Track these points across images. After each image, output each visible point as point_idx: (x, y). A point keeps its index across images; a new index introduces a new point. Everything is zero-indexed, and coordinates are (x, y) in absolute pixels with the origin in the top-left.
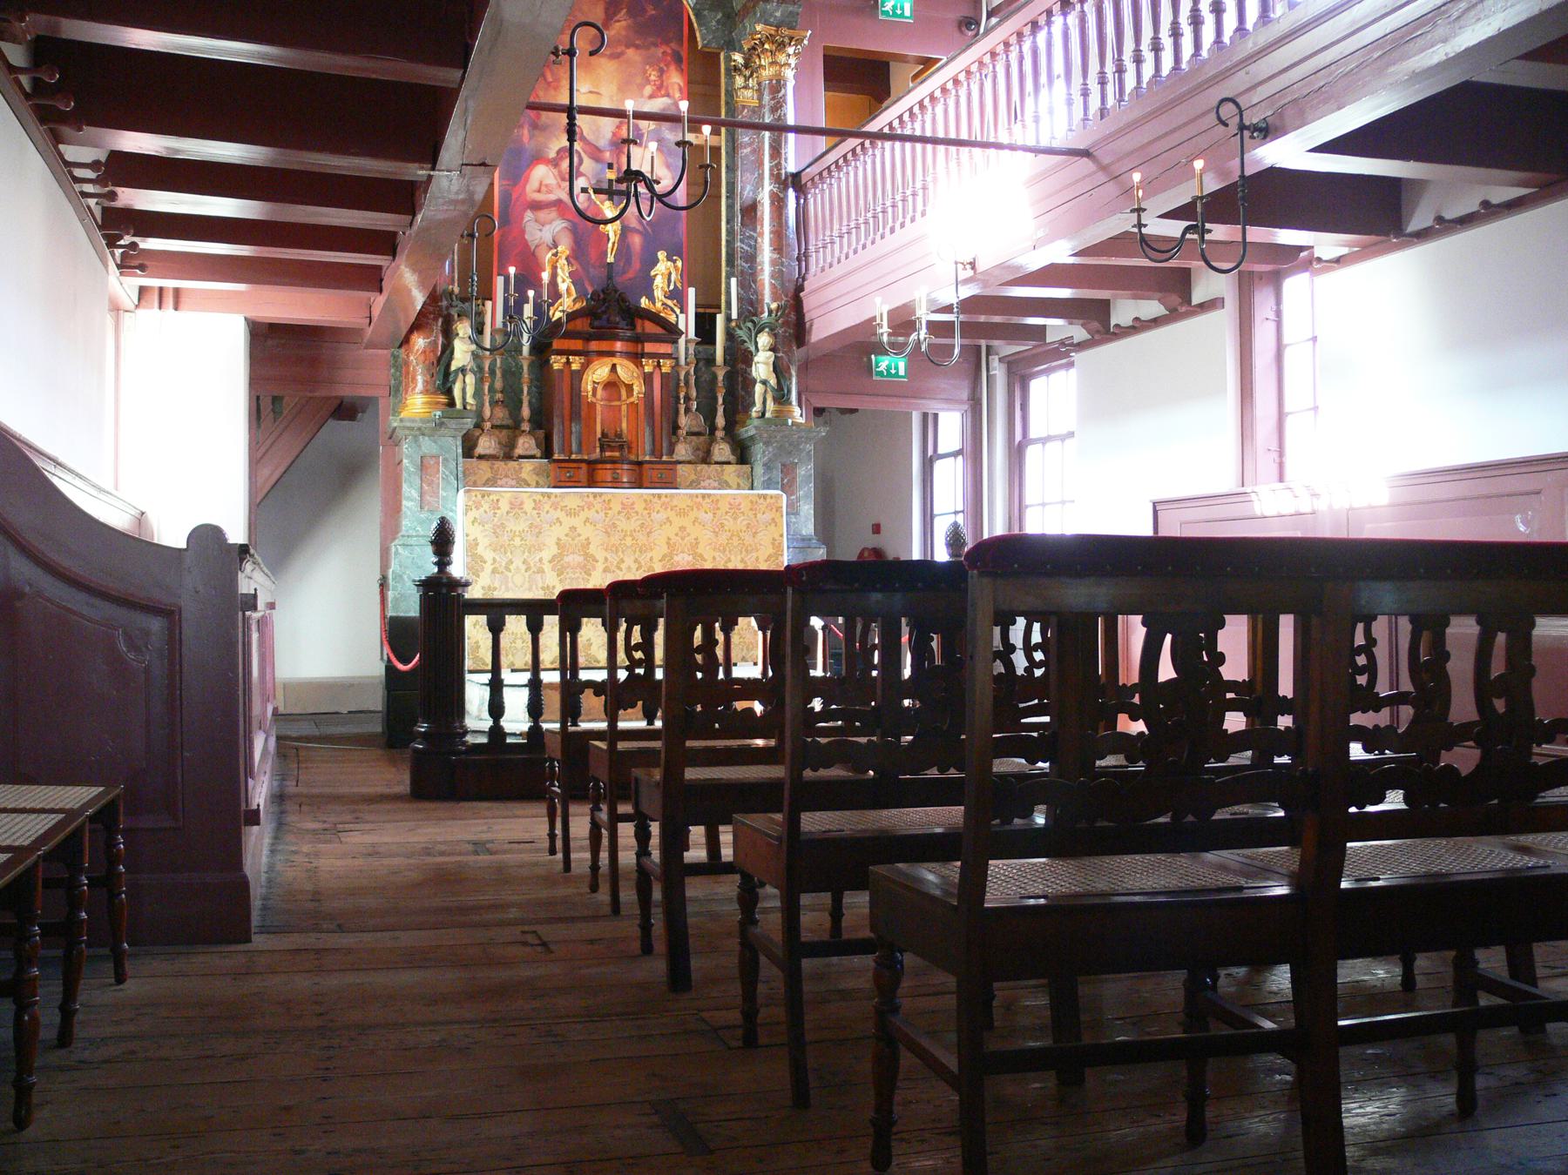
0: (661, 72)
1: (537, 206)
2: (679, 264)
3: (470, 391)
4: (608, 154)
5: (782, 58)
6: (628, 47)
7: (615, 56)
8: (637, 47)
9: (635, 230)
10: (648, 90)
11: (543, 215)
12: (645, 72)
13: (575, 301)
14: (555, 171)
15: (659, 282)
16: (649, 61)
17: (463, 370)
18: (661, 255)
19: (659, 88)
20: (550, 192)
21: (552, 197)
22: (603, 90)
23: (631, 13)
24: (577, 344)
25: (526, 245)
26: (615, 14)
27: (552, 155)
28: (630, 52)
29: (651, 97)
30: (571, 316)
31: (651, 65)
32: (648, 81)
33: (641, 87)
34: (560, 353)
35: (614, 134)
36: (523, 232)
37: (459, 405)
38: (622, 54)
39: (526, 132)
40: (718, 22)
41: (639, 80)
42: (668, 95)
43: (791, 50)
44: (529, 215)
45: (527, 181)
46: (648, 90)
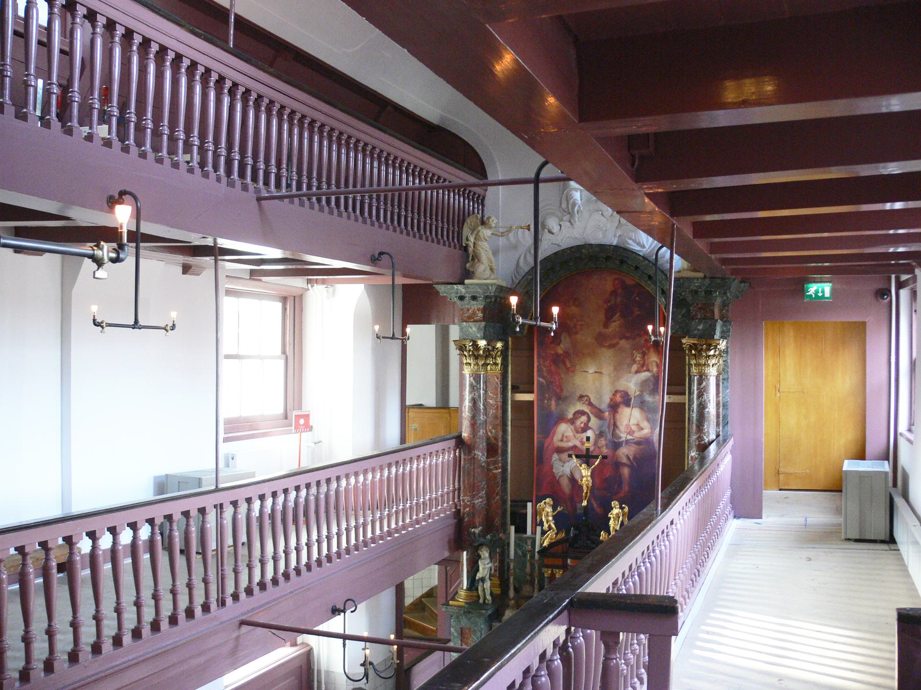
0: (644, 354)
1: (560, 450)
2: (626, 509)
3: (488, 592)
4: (607, 414)
5: (702, 361)
6: (621, 339)
7: (612, 346)
8: (627, 338)
9: (624, 465)
10: (635, 367)
11: (565, 456)
12: (632, 355)
13: (557, 534)
14: (572, 427)
15: (611, 523)
16: (636, 348)
17: (483, 580)
18: (615, 503)
19: (643, 366)
20: (568, 441)
21: (570, 444)
22: (604, 371)
23: (623, 316)
24: (559, 562)
25: (553, 475)
26: (612, 318)
27: (570, 416)
28: (623, 343)
29: (637, 372)
30: (551, 545)
31: (637, 350)
32: (634, 361)
33: (630, 366)
34: (547, 567)
35: (611, 400)
36: (552, 467)
37: (481, 601)
38: (617, 343)
39: (553, 402)
40: (683, 316)
41: (628, 361)
42: (648, 370)
43: (712, 353)
44: (555, 456)
45: (554, 433)
46: (635, 367)
